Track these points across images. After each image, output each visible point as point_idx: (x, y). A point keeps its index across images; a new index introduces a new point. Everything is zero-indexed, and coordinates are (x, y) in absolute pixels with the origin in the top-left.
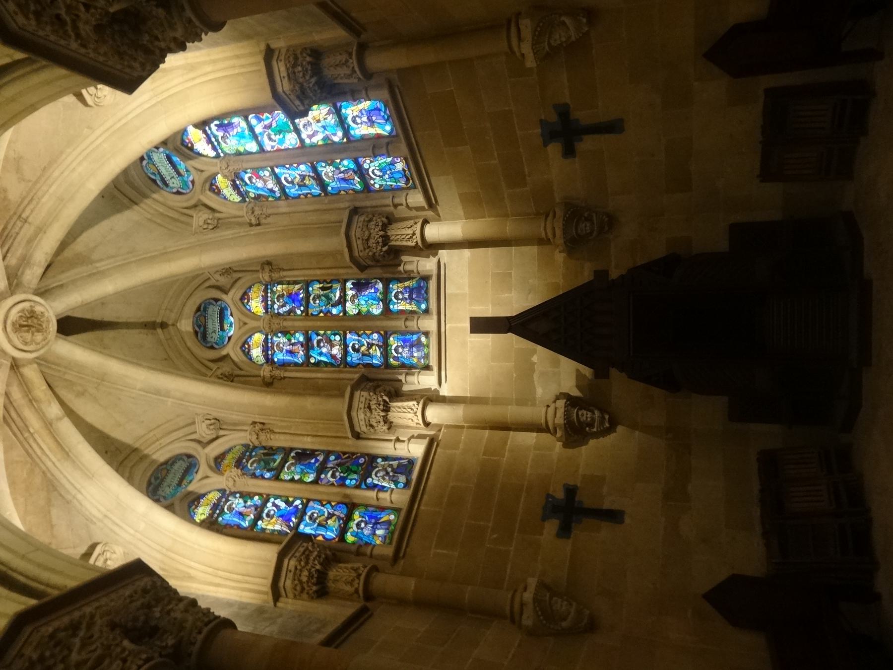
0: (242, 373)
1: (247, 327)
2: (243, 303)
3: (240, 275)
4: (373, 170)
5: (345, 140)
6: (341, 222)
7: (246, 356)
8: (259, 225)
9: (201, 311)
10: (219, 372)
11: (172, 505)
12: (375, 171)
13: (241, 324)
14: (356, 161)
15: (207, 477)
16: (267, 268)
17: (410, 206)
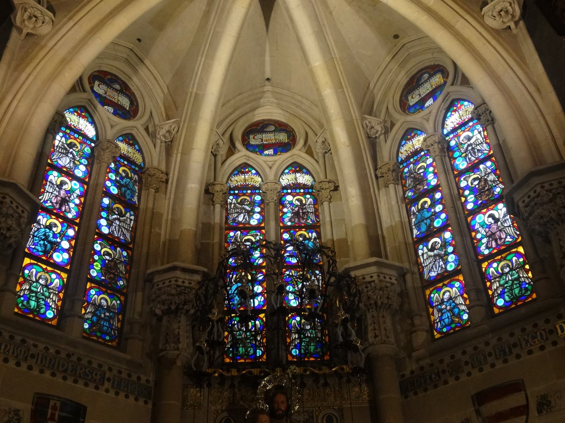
0: (219, 164)
1: (267, 170)
2: (291, 165)
3: (321, 161)
4: (449, 291)
5: (480, 258)
6: (387, 258)
7: (236, 169)
8: (377, 177)
9: (281, 127)
10: (221, 142)
11: (84, 91)
12: (448, 294)
13: (270, 165)
14: (456, 272)
15: (112, 127)
16: (332, 186)
17: (414, 335)
